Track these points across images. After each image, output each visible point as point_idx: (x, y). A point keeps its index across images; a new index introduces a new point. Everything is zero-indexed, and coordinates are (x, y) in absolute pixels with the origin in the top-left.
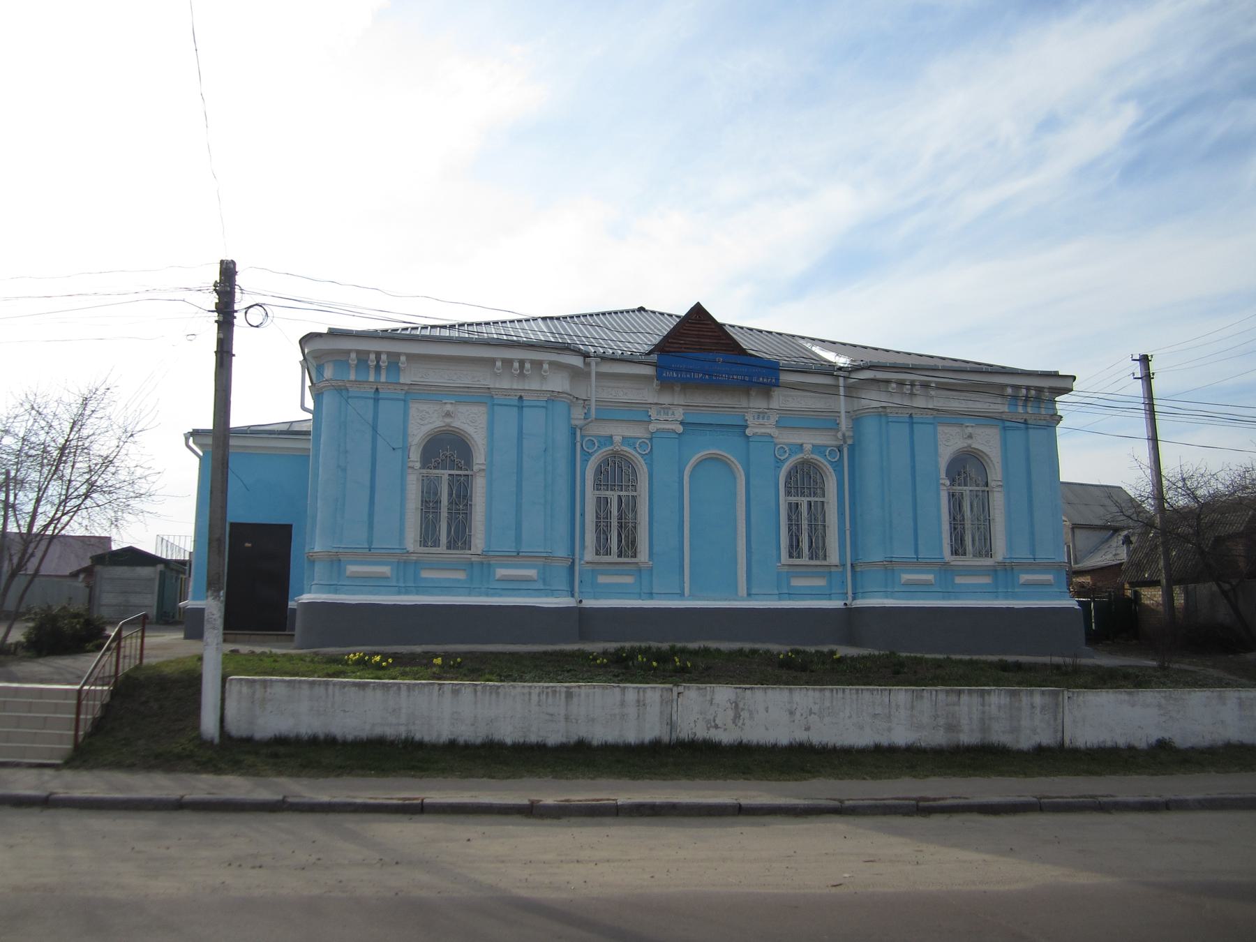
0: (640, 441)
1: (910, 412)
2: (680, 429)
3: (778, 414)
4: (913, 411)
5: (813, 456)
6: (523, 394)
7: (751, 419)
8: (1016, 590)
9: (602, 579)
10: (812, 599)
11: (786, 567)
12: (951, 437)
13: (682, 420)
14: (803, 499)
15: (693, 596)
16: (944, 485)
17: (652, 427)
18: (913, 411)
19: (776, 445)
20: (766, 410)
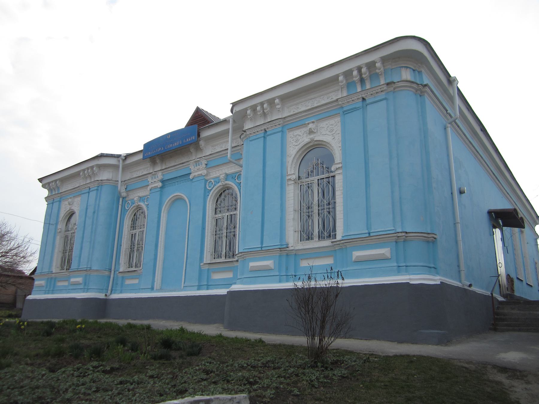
0: (147, 197)
1: (263, 128)
2: (160, 184)
3: (205, 159)
4: (265, 127)
5: (227, 182)
6: (89, 186)
7: (193, 167)
8: (348, 269)
9: (128, 282)
10: (216, 288)
11: (207, 266)
12: (300, 137)
13: (163, 179)
14: (224, 215)
15: (161, 290)
16: (290, 180)
17: (149, 188)
18: (265, 127)
19: (206, 181)
20: (198, 159)
